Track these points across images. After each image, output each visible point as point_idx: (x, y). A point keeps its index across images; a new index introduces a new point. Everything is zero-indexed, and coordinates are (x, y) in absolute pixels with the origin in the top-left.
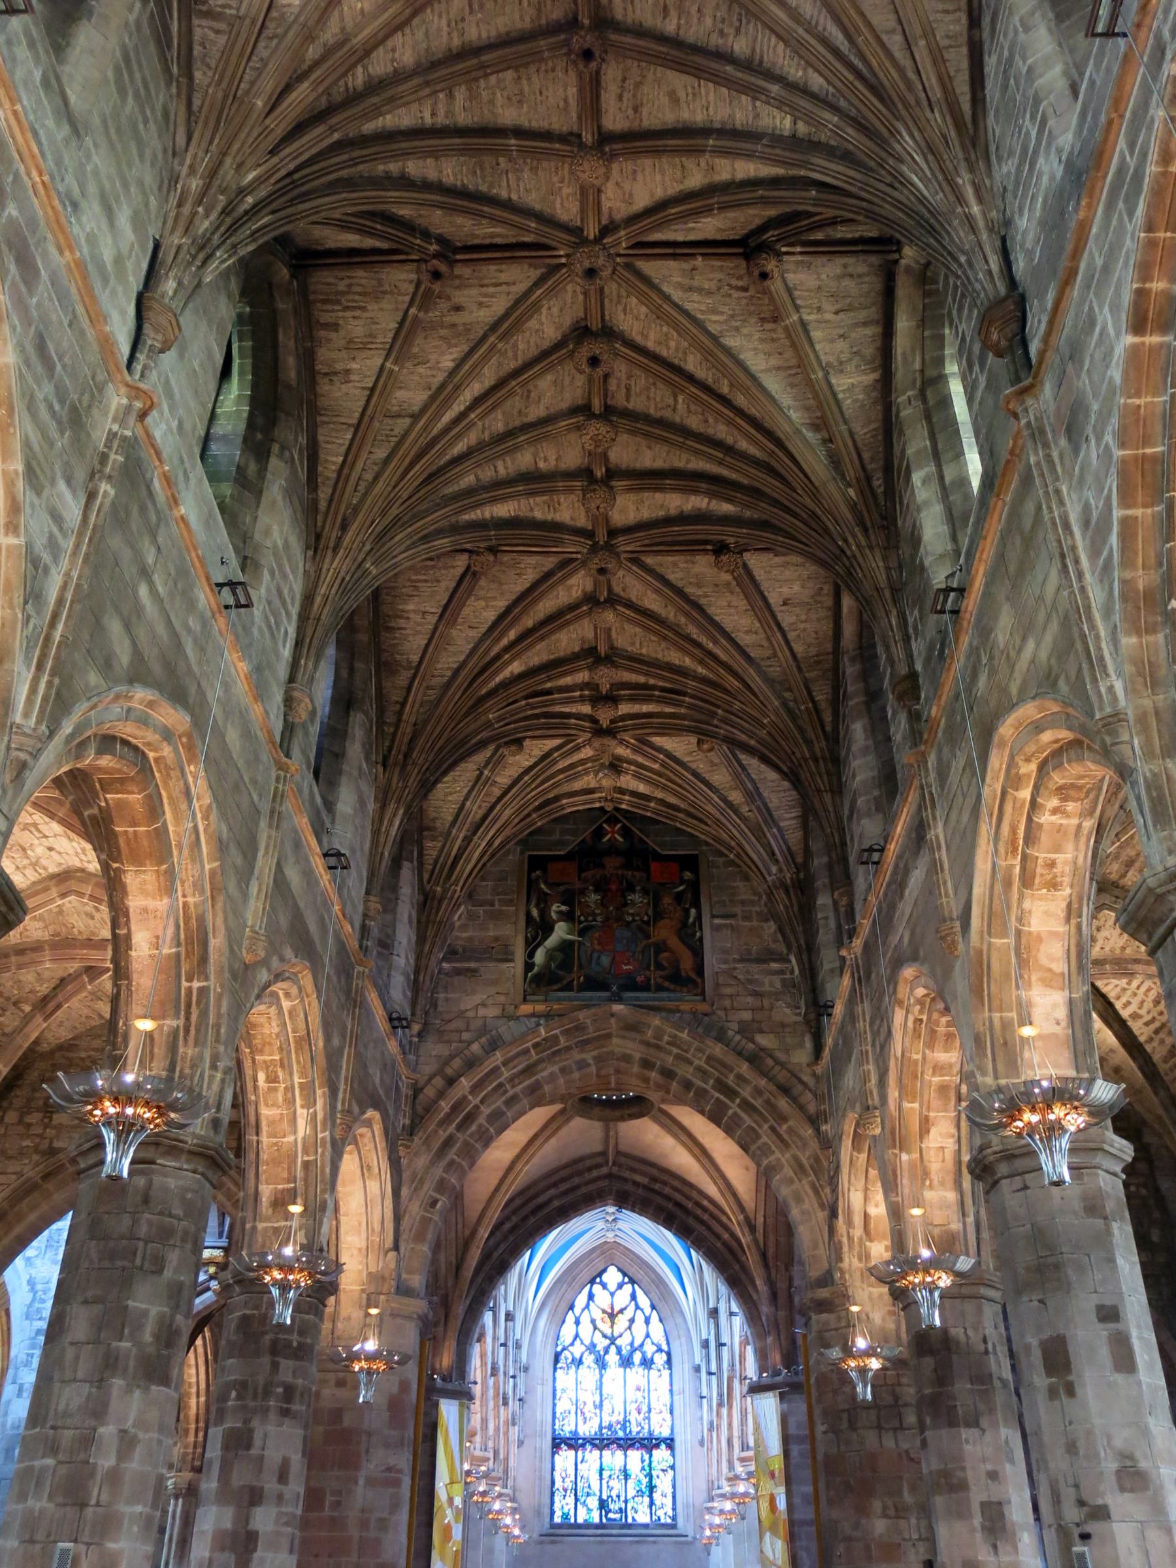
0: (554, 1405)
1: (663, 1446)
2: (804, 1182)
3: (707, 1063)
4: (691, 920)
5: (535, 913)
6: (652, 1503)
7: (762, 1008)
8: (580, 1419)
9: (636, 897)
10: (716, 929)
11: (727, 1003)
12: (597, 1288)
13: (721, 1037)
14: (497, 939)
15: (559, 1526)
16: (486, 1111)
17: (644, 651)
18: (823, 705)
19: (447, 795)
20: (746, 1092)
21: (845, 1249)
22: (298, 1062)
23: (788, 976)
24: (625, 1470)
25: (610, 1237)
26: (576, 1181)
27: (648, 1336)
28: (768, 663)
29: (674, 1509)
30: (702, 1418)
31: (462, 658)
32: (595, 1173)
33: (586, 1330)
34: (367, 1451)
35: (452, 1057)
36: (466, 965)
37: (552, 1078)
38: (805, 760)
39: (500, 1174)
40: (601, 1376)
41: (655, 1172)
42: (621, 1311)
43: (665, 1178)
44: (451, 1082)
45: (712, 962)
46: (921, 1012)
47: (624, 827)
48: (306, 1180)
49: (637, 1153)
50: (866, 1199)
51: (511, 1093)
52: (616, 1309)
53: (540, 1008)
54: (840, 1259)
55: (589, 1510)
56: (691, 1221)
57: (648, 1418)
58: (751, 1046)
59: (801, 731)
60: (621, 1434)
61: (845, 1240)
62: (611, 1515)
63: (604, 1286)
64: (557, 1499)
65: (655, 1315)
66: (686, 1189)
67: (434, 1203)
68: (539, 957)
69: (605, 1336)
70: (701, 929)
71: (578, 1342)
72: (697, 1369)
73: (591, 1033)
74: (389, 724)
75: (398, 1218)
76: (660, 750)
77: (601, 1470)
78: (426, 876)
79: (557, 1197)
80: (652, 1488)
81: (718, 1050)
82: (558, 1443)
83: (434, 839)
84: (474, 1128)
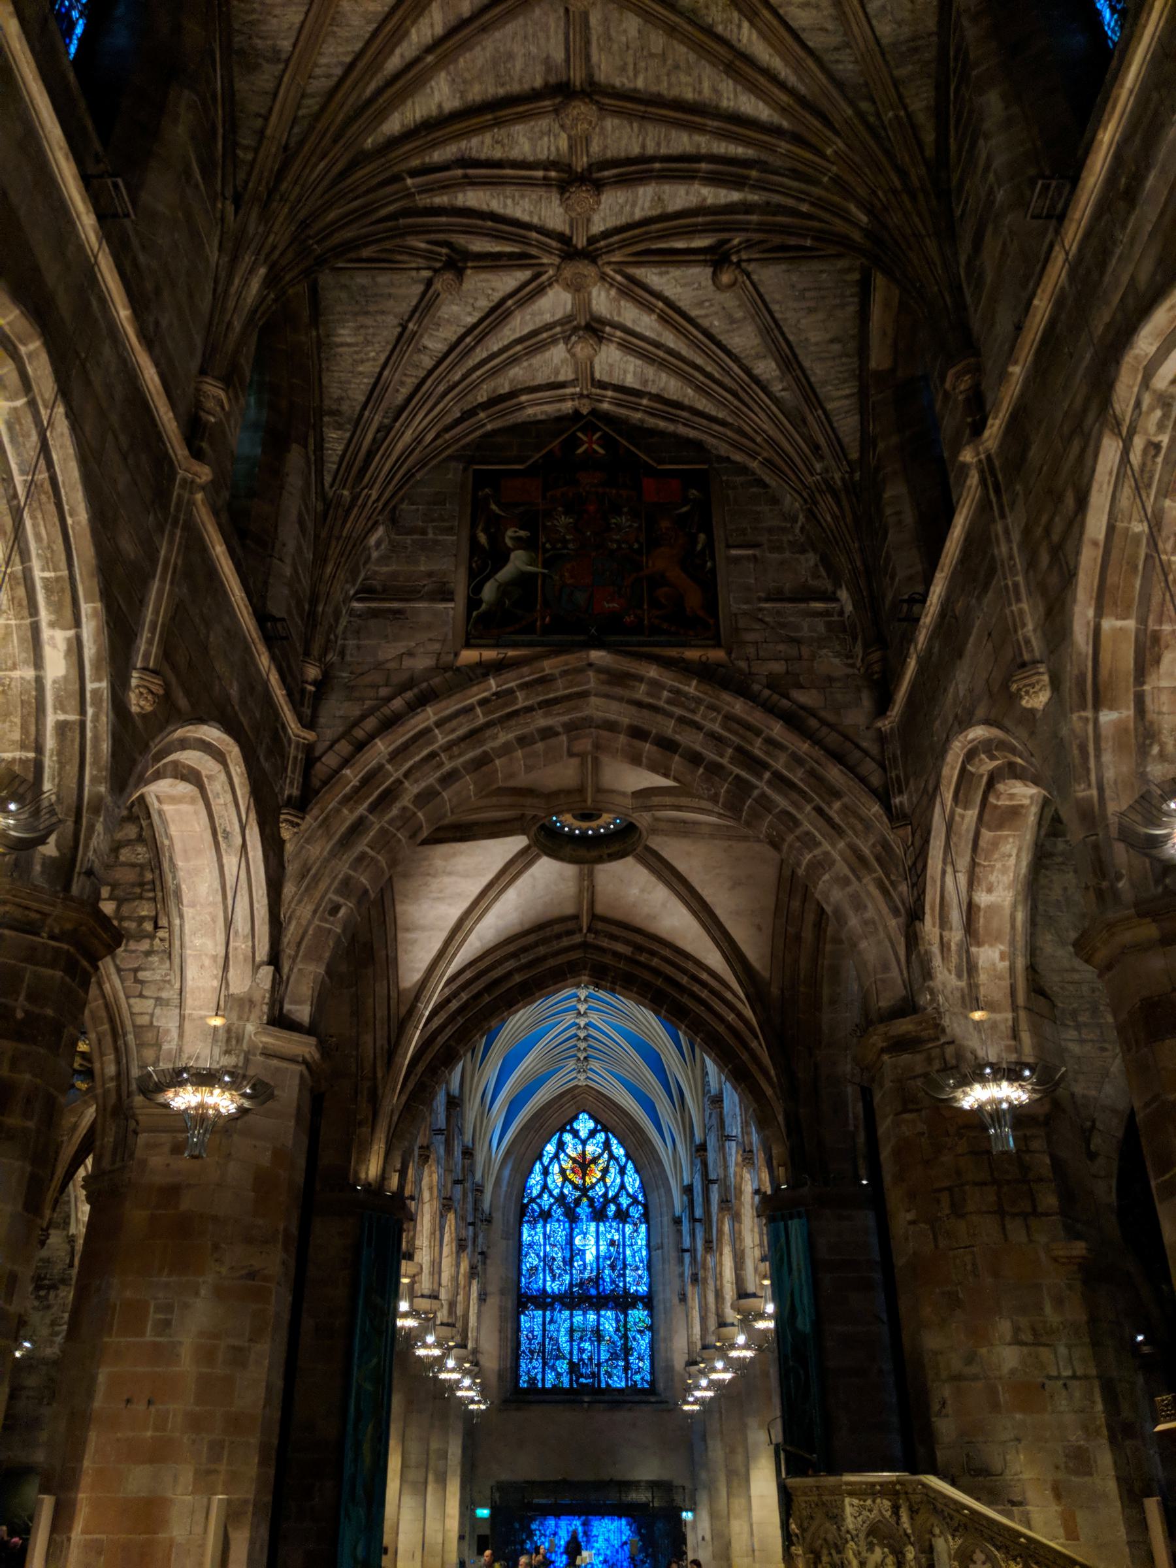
0: (520, 1262)
1: (640, 1306)
2: (867, 880)
3: (724, 726)
4: (699, 547)
5: (483, 538)
6: (627, 1368)
7: (800, 658)
8: (548, 1278)
9: (624, 520)
10: (737, 560)
11: (751, 650)
13: (743, 690)
14: (430, 574)
15: (526, 1391)
16: (413, 789)
17: (640, 83)
18: (921, 118)
19: (356, 363)
20: (779, 764)
21: (937, 962)
22: (38, 537)
23: (836, 618)
24: (598, 1330)
25: (582, 1080)
26: (542, 950)
27: (622, 1186)
28: (836, 56)
29: (652, 1373)
30: (682, 1275)
31: (358, 46)
32: (565, 942)
33: (555, 1180)
34: (216, 1247)
35: (363, 717)
36: (387, 605)
37: (506, 749)
38: (894, 192)
39: (443, 935)
40: (572, 1229)
41: (639, 939)
42: (595, 1160)
43: (655, 946)
44: (360, 746)
45: (731, 602)
46: (1161, 427)
47: (605, 436)
48: (60, 752)
49: (619, 916)
50: (972, 882)
51: (448, 766)
52: (589, 1157)
53: (490, 654)
54: (928, 974)
55: (559, 1375)
56: (686, 1000)
57: (624, 1275)
58: (785, 702)
59: (888, 153)
60: (593, 1292)
61: (935, 949)
62: (583, 1380)
63: (576, 1134)
64: (523, 1365)
65: (630, 1166)
66: (679, 960)
67: (335, 909)
68: (488, 592)
69: (576, 1187)
70: (713, 559)
71: (545, 1196)
72: (677, 1221)
73: (560, 689)
74: (246, 148)
75: (276, 925)
76: (659, 296)
77: (571, 1331)
78: (328, 479)
79: (519, 969)
80: (627, 1351)
81: (738, 707)
82: (524, 1301)
83: (339, 427)
84: (395, 811)
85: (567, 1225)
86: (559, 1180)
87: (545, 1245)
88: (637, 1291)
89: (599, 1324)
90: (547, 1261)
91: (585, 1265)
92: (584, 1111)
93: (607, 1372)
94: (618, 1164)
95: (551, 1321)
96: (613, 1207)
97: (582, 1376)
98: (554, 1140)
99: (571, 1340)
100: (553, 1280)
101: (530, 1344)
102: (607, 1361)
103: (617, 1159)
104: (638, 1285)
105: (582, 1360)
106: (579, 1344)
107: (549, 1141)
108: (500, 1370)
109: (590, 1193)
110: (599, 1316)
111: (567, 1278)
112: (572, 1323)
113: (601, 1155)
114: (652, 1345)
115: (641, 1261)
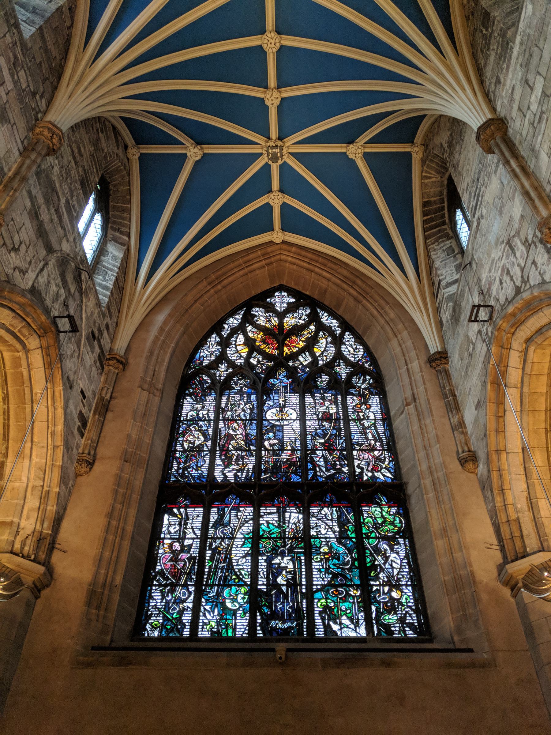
8: (218, 461)
27: (339, 355)
40: (261, 403)
57: (350, 459)
60: (295, 478)
63: (270, 308)
64: (157, 595)
69: (267, 357)
71: (223, 367)
85: (253, 397)
88: (373, 477)
89: (307, 527)
91: (281, 442)
92: (281, 288)
93: (326, 608)
95: (219, 523)
97: (274, 615)
98: (239, 316)
99: (255, 553)
100: (227, 463)
101: (175, 559)
102: (324, 588)
103: (328, 330)
104: (374, 470)
105: (278, 586)
106: (269, 561)
107: (232, 314)
108: (94, 583)
110: (307, 515)
111: (251, 462)
112: (257, 526)
115: (378, 439)
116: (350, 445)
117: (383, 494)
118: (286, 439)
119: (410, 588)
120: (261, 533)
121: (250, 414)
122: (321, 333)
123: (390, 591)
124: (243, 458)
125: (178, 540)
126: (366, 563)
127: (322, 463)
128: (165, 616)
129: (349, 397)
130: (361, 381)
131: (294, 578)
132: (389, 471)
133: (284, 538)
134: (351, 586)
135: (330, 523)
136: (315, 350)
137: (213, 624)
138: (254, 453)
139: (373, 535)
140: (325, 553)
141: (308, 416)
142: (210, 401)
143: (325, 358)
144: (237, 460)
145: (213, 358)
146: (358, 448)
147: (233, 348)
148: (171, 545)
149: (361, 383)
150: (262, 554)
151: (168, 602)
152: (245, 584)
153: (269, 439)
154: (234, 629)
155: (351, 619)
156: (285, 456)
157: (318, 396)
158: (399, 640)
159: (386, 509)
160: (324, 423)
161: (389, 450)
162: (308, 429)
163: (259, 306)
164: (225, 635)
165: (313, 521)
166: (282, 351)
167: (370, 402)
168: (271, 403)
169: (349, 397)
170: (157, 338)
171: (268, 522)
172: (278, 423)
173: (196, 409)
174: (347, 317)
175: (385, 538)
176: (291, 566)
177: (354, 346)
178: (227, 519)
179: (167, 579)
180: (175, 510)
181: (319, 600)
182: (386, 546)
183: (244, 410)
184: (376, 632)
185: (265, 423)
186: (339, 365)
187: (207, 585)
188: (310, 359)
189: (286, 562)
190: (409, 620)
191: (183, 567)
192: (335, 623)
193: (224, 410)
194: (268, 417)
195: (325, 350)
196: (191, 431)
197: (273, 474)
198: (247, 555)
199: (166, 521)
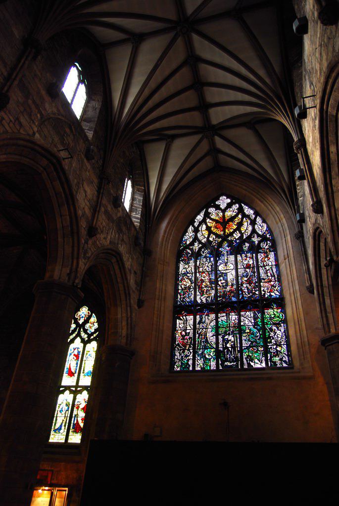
0: (177, 285)
8: (198, 293)
12: (212, 210)
27: (254, 231)
33: (203, 235)
40: (216, 262)
57: (260, 287)
60: (234, 299)
63: (218, 207)
64: (177, 354)
65: (259, 220)
69: (217, 236)
71: (196, 244)
77: (217, 327)
80: (266, 340)
82: (181, 309)
85: (212, 259)
86: (206, 233)
87: (196, 273)
88: (271, 295)
90: (197, 284)
91: (226, 281)
92: (222, 195)
93: (248, 356)
94: (250, 219)
95: (200, 322)
96: (247, 245)
97: (227, 360)
98: (202, 214)
99: (217, 335)
101: (183, 339)
102: (248, 348)
103: (248, 217)
104: (271, 291)
106: (223, 337)
107: (198, 214)
109: (229, 239)
110: (240, 316)
112: (217, 322)
113: (236, 216)
114: (286, 333)
116: (260, 280)
117: (275, 303)
118: (229, 280)
119: (285, 346)
120: (219, 325)
121: (211, 268)
122: (245, 219)
123: (276, 347)
124: (209, 291)
125: (184, 331)
126: (266, 335)
127: (246, 291)
128: (181, 362)
129: (259, 254)
130: (265, 245)
131: (234, 344)
132: (278, 291)
133: (230, 327)
134: (259, 346)
135: (250, 319)
136: (242, 229)
137: (202, 365)
138: (214, 288)
139: (269, 323)
140: (248, 333)
141: (239, 267)
142: (192, 263)
143: (246, 234)
144: (206, 292)
145: (191, 240)
146: (263, 281)
147: (200, 233)
148: (181, 333)
149: (264, 245)
150: (220, 335)
151: (182, 357)
152: (214, 348)
153: (221, 280)
154: (210, 366)
155: (259, 360)
156: (228, 289)
157: (243, 255)
158: (279, 368)
159: (276, 310)
160: (247, 270)
161: (278, 281)
162: (239, 274)
163: (212, 207)
164: (206, 369)
165: (242, 318)
166: (225, 232)
167: (269, 256)
168: (221, 261)
169: (259, 254)
170: (164, 236)
171: (222, 320)
172: (224, 272)
173: (186, 268)
174: (258, 209)
175: (274, 324)
176: (233, 339)
177: (262, 225)
178: (204, 320)
179: (181, 347)
180: (181, 317)
181: (245, 353)
182: (275, 328)
183: (208, 267)
184: (269, 365)
185: (219, 272)
186: (254, 237)
187: (197, 349)
188: (239, 235)
189: (231, 338)
190: (284, 359)
191: (187, 342)
192: (252, 362)
193: (198, 267)
194: (220, 269)
195: (247, 229)
196: (184, 279)
197: (223, 298)
198: (213, 335)
199: (178, 323)
